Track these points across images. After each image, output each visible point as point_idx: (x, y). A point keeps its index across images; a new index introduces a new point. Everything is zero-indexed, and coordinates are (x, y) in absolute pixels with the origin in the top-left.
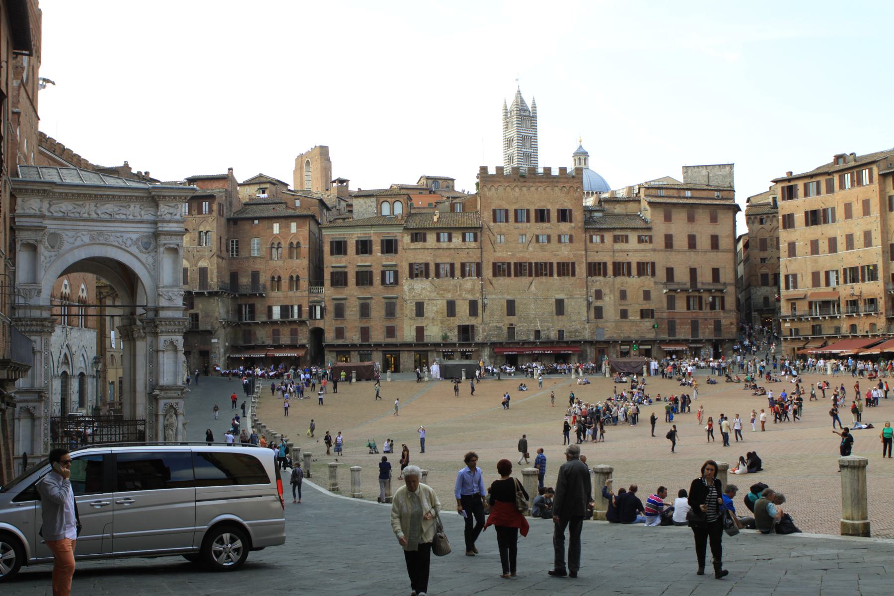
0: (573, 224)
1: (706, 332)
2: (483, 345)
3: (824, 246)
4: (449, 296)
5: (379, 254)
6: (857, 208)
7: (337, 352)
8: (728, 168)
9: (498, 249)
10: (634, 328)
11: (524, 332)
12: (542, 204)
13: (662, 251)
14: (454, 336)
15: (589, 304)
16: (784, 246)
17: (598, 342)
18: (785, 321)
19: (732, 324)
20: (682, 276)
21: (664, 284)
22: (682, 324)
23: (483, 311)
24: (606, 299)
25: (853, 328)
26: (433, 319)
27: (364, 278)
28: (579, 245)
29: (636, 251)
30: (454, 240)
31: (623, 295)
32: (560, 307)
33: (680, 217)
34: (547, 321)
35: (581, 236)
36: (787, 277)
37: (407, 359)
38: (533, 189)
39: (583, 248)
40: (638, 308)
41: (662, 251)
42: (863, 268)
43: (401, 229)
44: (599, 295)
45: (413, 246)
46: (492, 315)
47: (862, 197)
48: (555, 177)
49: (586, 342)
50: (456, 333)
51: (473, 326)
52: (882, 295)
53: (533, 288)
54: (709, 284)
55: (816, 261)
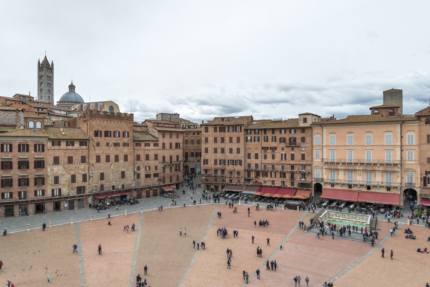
0: (129, 138)
1: (174, 181)
2: (89, 195)
3: (219, 150)
4: (72, 173)
5: (33, 152)
6: (234, 140)
7: (5, 206)
8: (177, 116)
9: (96, 149)
11: (108, 187)
12: (117, 129)
14: (74, 193)
15: (135, 173)
16: (203, 149)
18: (203, 176)
20: (167, 159)
22: (168, 178)
23: (89, 179)
24: (142, 170)
25: (231, 181)
26: (64, 184)
27: (24, 164)
28: (131, 147)
29: (153, 150)
30: (75, 145)
32: (123, 174)
33: (167, 136)
34: (118, 181)
35: (131, 143)
36: (204, 160)
37: (49, 206)
39: (133, 149)
42: (236, 160)
43: (46, 139)
44: (139, 168)
45: (53, 148)
46: (93, 180)
47: (237, 136)
50: (76, 191)
51: (84, 187)
53: (112, 166)
55: (216, 156)
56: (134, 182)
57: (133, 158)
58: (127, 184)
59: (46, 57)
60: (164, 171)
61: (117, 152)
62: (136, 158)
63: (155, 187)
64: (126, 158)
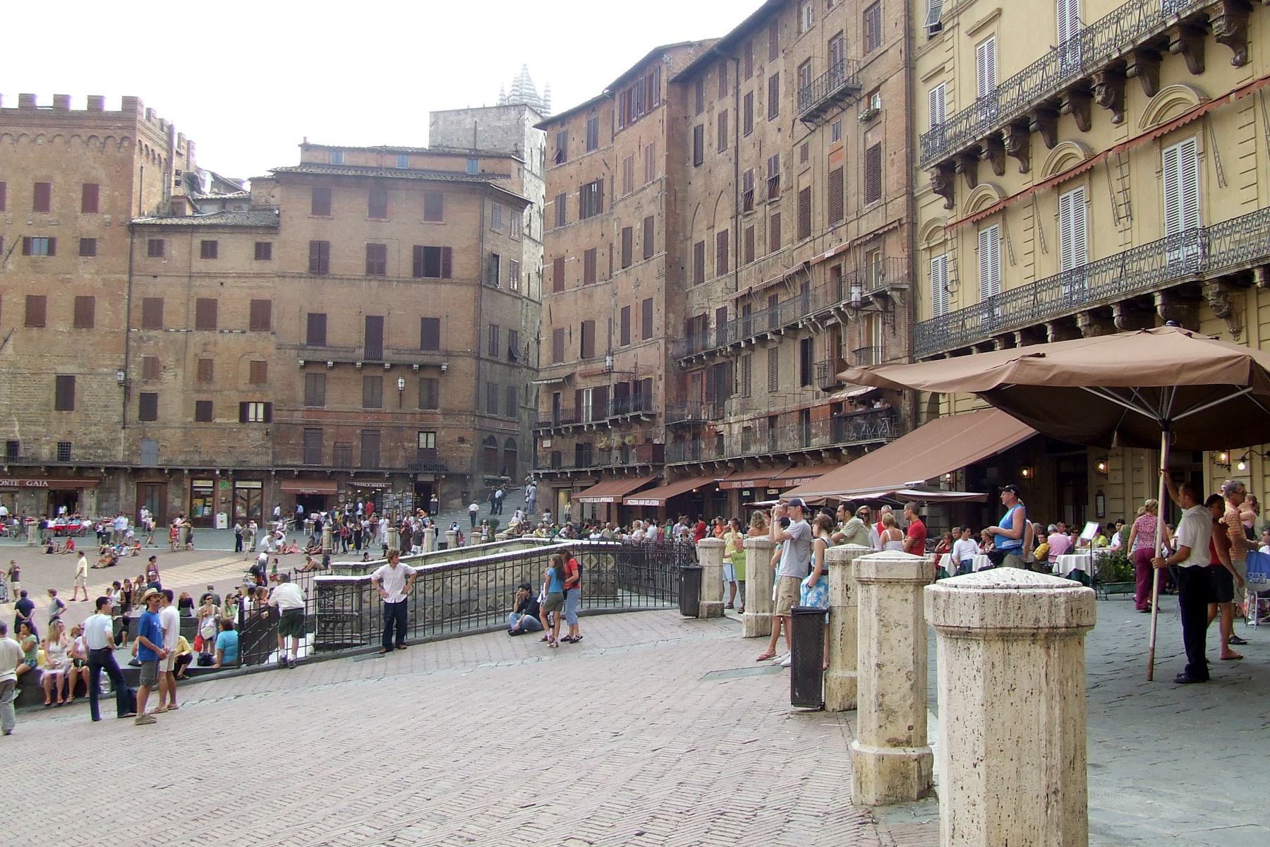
10: (224, 443)
13: (300, 276)
15: (126, 386)
17: (137, 472)
19: (462, 440)
20: (345, 332)
21: (301, 348)
24: (167, 376)
29: (240, 276)
31: (205, 370)
32: (65, 391)
38: (23, 140)
40: (237, 399)
41: (300, 276)
44: (152, 368)
48: (79, 115)
49: (112, 470)
52: (661, 372)
54: (411, 352)
56: (122, 435)
57: (123, 315)
58: (86, 442)
59: (525, 67)
60: (314, 399)
61: (36, 284)
62: (138, 314)
63: (240, 475)
64: (84, 314)
